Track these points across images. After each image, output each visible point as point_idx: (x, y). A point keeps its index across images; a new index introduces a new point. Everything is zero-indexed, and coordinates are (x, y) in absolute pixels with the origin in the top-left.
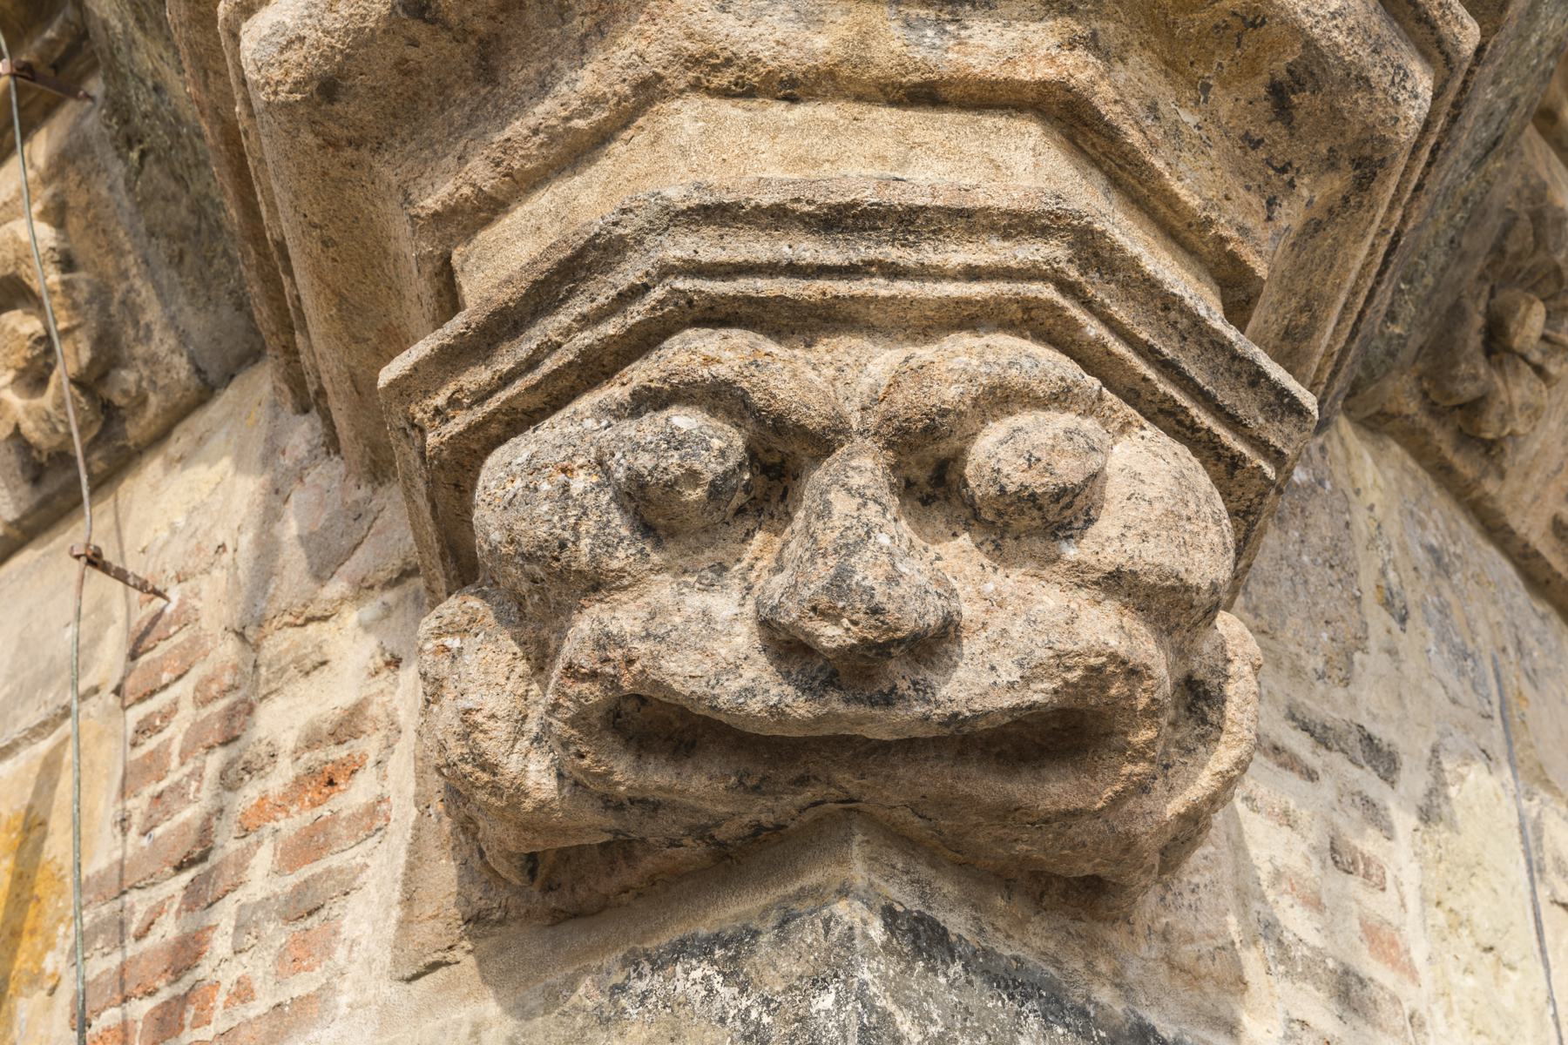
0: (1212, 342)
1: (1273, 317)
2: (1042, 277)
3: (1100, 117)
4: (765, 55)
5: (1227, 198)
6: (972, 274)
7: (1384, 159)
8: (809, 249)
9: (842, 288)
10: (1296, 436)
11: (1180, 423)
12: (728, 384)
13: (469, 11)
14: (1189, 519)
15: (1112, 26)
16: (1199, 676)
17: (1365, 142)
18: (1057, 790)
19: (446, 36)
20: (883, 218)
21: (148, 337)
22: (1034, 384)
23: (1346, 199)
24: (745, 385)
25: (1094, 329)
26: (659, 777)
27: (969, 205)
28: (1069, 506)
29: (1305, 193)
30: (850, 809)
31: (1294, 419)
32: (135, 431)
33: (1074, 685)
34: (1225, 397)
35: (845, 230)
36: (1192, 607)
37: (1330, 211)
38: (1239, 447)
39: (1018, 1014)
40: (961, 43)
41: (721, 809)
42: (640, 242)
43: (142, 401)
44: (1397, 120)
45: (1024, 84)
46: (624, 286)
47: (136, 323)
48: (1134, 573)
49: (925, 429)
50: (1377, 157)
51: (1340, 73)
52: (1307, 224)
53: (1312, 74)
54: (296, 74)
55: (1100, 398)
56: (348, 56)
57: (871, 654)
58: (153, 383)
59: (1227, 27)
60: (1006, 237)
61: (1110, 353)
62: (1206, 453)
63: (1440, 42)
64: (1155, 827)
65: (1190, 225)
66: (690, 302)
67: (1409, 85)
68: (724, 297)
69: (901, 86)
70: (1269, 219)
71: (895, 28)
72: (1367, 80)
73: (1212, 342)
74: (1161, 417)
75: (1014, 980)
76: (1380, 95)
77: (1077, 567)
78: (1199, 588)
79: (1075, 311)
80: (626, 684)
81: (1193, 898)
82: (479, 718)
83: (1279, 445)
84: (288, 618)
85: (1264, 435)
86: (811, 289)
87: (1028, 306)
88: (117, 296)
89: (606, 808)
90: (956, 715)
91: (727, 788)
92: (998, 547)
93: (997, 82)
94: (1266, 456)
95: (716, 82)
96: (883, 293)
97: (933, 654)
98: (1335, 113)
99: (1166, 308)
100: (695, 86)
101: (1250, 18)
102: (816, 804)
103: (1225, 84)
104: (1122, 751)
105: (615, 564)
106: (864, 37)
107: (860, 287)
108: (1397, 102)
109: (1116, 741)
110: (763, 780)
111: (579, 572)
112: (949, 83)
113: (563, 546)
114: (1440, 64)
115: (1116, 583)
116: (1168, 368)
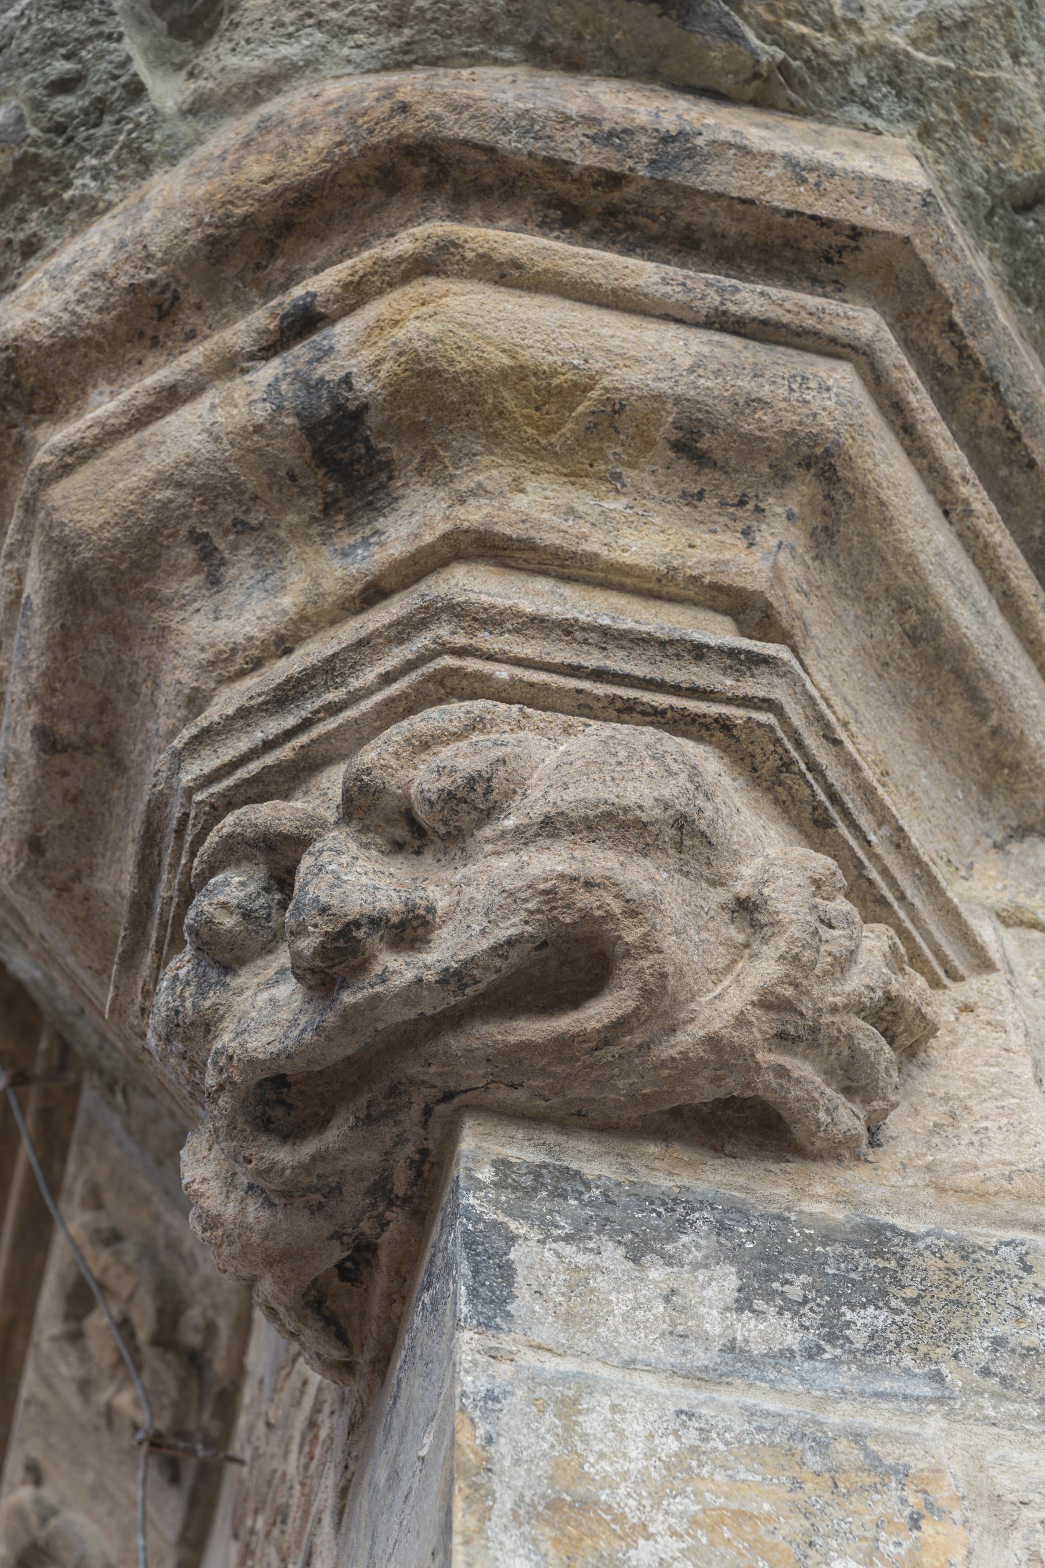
0: (632, 641)
1: (877, 630)
2: (436, 654)
3: (510, 538)
4: (255, 632)
5: (691, 546)
6: (387, 679)
7: (826, 450)
8: (273, 727)
9: (303, 739)
10: (777, 681)
11: (643, 713)
12: (230, 836)
13: (81, 728)
14: (620, 763)
15: (495, 472)
16: (743, 895)
17: (797, 445)
18: (597, 1013)
19: (79, 755)
20: (314, 677)
21: (195, 1265)
22: (446, 725)
23: (828, 497)
24: (239, 830)
25: (503, 672)
26: (310, 1148)
27: (363, 634)
28: (489, 791)
29: (779, 510)
30: (457, 1110)
31: (763, 668)
32: (219, 1365)
33: (539, 911)
34: (672, 674)
35: (294, 699)
36: (645, 825)
37: (825, 513)
38: (715, 709)
39: (681, 1221)
40: (381, 544)
41: (371, 1157)
42: (171, 788)
43: (210, 1330)
44: (815, 415)
45: (432, 545)
46: (174, 824)
47: (182, 1258)
48: (562, 813)
49: (360, 789)
50: (819, 451)
51: (725, 408)
52: (813, 534)
53: (700, 420)
54: (13, 849)
55: (526, 717)
56: (33, 812)
57: (341, 943)
58: (215, 1307)
59: (596, 425)
60: (401, 641)
61: (532, 685)
62: (694, 729)
63: (833, 340)
64: (732, 1021)
65: (659, 581)
66: (212, 806)
67: (813, 384)
68: (229, 789)
69: (353, 598)
70: (751, 545)
71: (336, 563)
72: (759, 400)
73: (632, 641)
74: (625, 717)
75: (674, 1200)
76: (782, 405)
77: (519, 831)
78: (640, 807)
79: (472, 665)
80: (237, 1079)
81: (976, 1139)
82: (195, 1186)
83: (761, 694)
84: (283, 1373)
85: (740, 693)
86: (285, 752)
87: (441, 678)
88: (161, 1243)
89: (312, 1213)
90: (447, 969)
91: (351, 1128)
92: (463, 850)
93: (413, 555)
94: (758, 708)
95: (234, 668)
96: (334, 725)
97: (428, 942)
98: (749, 439)
99: (568, 633)
100: (220, 682)
101: (609, 409)
102: (427, 1112)
103: (632, 465)
104: (627, 954)
105: (208, 1003)
106: (315, 582)
107: (315, 732)
108: (806, 402)
109: (619, 950)
110: (368, 1107)
111: (192, 1024)
112: (381, 576)
113: (177, 1012)
114: (853, 354)
115: (550, 827)
116: (599, 675)
